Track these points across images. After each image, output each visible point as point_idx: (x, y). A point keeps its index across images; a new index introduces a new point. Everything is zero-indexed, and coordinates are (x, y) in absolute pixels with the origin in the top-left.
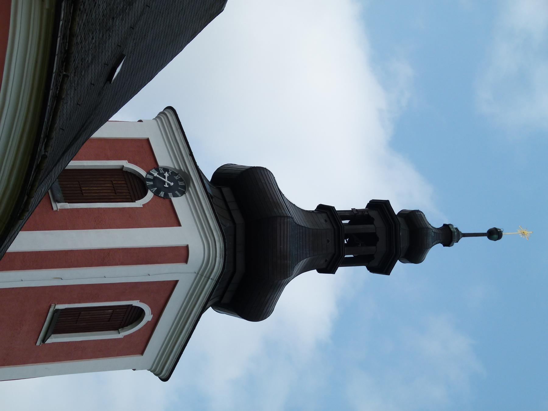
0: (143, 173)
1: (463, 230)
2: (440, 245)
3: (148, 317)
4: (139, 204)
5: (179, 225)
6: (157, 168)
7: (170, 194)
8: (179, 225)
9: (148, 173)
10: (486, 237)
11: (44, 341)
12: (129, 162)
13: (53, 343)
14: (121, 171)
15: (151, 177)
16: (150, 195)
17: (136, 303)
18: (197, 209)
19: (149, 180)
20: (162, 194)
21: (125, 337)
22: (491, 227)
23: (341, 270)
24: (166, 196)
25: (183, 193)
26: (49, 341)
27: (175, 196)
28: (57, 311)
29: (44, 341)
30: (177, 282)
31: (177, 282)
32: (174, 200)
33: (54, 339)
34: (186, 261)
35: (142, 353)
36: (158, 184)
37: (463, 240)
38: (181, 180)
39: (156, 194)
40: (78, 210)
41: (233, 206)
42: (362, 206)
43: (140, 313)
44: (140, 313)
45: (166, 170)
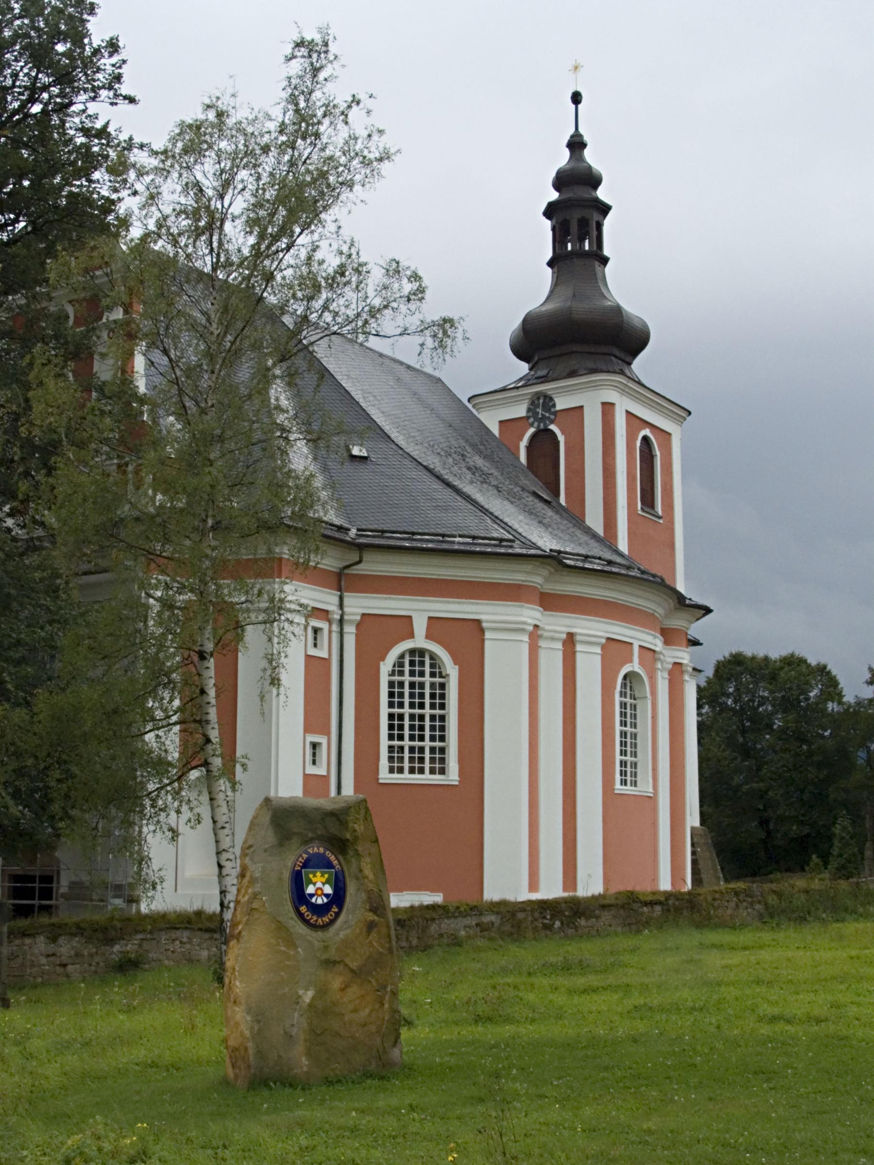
0: (532, 430)
1: (572, 131)
2: (587, 153)
3: (646, 432)
4: (561, 438)
5: (581, 407)
6: (528, 418)
7: (553, 410)
8: (581, 407)
9: (532, 425)
10: (580, 106)
11: (660, 518)
12: (521, 440)
13: (662, 510)
14: (529, 448)
15: (536, 424)
16: (552, 427)
18: (567, 390)
19: (539, 426)
20: (552, 417)
21: (659, 450)
23: (606, 252)
24: (556, 413)
25: (551, 399)
26: (660, 513)
27: (554, 406)
28: (642, 509)
29: (660, 518)
30: (628, 412)
31: (628, 412)
32: (558, 408)
34: (613, 405)
35: (670, 434)
37: (581, 130)
38: (538, 399)
39: (552, 422)
40: (566, 488)
42: (548, 224)
43: (645, 439)
44: (645, 439)
45: (529, 410)
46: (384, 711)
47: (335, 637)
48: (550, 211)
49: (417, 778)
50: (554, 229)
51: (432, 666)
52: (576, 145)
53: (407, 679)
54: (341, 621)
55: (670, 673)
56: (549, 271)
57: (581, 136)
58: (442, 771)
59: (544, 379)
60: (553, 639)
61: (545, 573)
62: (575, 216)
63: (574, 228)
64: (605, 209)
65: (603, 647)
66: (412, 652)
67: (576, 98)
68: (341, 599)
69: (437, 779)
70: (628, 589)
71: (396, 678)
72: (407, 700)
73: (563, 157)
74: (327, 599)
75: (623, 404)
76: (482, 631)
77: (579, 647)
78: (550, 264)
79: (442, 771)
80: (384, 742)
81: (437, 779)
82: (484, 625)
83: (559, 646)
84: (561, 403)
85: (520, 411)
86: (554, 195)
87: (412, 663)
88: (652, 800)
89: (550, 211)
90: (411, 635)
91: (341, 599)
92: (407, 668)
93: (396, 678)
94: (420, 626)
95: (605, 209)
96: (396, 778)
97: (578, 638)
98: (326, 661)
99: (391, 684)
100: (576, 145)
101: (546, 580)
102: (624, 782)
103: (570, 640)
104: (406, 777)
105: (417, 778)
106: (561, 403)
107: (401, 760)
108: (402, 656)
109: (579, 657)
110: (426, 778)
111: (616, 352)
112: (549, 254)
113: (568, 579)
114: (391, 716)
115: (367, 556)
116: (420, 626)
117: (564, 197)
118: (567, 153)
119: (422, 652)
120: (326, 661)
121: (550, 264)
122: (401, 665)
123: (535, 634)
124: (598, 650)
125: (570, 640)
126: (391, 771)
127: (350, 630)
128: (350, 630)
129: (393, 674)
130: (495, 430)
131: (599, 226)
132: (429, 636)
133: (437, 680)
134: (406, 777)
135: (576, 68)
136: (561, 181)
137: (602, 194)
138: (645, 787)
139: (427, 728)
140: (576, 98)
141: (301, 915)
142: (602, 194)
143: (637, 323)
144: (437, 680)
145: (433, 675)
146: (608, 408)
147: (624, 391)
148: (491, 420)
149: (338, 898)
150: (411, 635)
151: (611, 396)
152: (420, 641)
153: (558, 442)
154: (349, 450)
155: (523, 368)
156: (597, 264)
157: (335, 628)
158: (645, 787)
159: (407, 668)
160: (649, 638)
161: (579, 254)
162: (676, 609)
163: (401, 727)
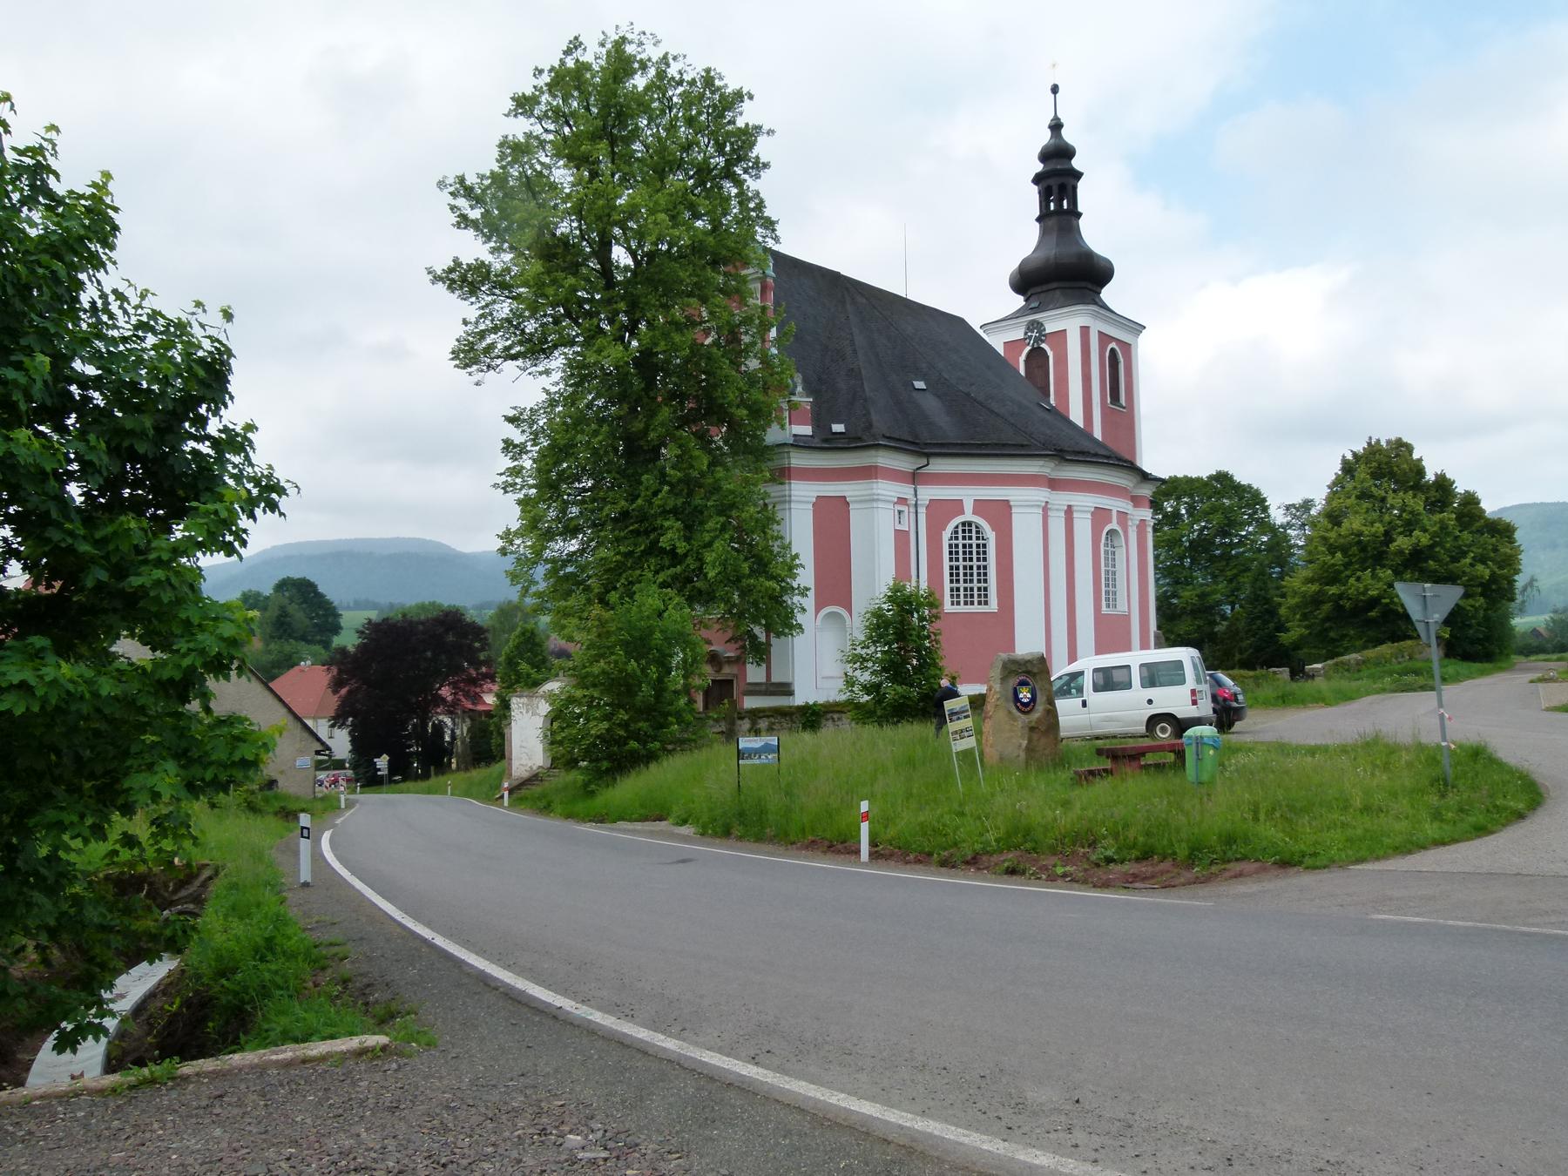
0: (1029, 348)
1: (1052, 116)
2: (1063, 131)
3: (1113, 345)
4: (1050, 354)
14: (1027, 361)
16: (1043, 346)
17: (1107, 354)
22: (1050, 92)
23: (1080, 209)
24: (1044, 336)
25: (1042, 325)
27: (1045, 330)
32: (1047, 332)
33: (1123, 401)
34: (1088, 327)
36: (1037, 340)
37: (1059, 115)
39: (1043, 341)
41: (1045, 287)
42: (1035, 189)
43: (1113, 350)
44: (1113, 351)
45: (1026, 333)
46: (946, 564)
47: (913, 516)
48: (1037, 179)
49: (969, 609)
50: (1040, 193)
51: (978, 532)
52: (1056, 127)
53: (960, 542)
54: (916, 505)
55: (1138, 527)
56: (1037, 225)
57: (1059, 119)
58: (986, 603)
59: (1035, 310)
60: (1057, 510)
61: (1052, 465)
62: (1054, 182)
63: (1055, 189)
64: (1078, 175)
65: (1093, 514)
66: (964, 524)
67: (1055, 89)
68: (916, 491)
69: (983, 609)
70: (1106, 472)
71: (954, 542)
72: (961, 556)
73: (1045, 137)
74: (906, 490)
75: (1096, 326)
76: (1010, 507)
77: (1075, 515)
78: (1038, 220)
79: (986, 603)
80: (947, 586)
81: (983, 609)
82: (1012, 503)
83: (1063, 514)
84: (1050, 328)
85: (1018, 334)
86: (1039, 167)
87: (964, 531)
88: (1126, 618)
89: (1037, 179)
90: (963, 513)
91: (916, 491)
92: (960, 535)
93: (954, 542)
94: (968, 506)
95: (1078, 175)
96: (956, 609)
97: (1075, 508)
98: (907, 533)
99: (950, 546)
100: (1056, 127)
101: (1053, 470)
102: (1108, 606)
103: (1069, 511)
104: (962, 609)
105: (969, 609)
106: (1050, 328)
107: (958, 596)
108: (957, 527)
109: (1075, 521)
110: (976, 608)
111: (1090, 286)
112: (1036, 211)
113: (1065, 468)
114: (951, 568)
115: (932, 461)
116: (968, 506)
117: (1048, 168)
118: (1048, 133)
119: (970, 524)
120: (907, 533)
121: (1038, 220)
122: (956, 532)
123: (1045, 509)
124: (1089, 516)
125: (1069, 511)
126: (953, 604)
127: (922, 511)
128: (922, 511)
129: (951, 539)
130: (1001, 350)
131: (1075, 188)
132: (974, 513)
133: (981, 542)
134: (962, 609)
135: (1054, 66)
136: (1045, 156)
137: (1076, 163)
138: (1122, 607)
139: (975, 574)
140: (1055, 89)
141: (1017, 708)
142: (1076, 163)
143: (1103, 263)
144: (981, 542)
145: (978, 538)
146: (1085, 331)
147: (1096, 316)
148: (997, 342)
149: (1033, 699)
150: (963, 513)
151: (1083, 320)
152: (968, 516)
153: (1048, 357)
154: (913, 385)
155: (1019, 301)
156: (1073, 218)
157: (912, 510)
158: (1122, 607)
159: (960, 535)
160: (1124, 505)
161: (1059, 211)
162: (1142, 482)
163: (958, 575)
